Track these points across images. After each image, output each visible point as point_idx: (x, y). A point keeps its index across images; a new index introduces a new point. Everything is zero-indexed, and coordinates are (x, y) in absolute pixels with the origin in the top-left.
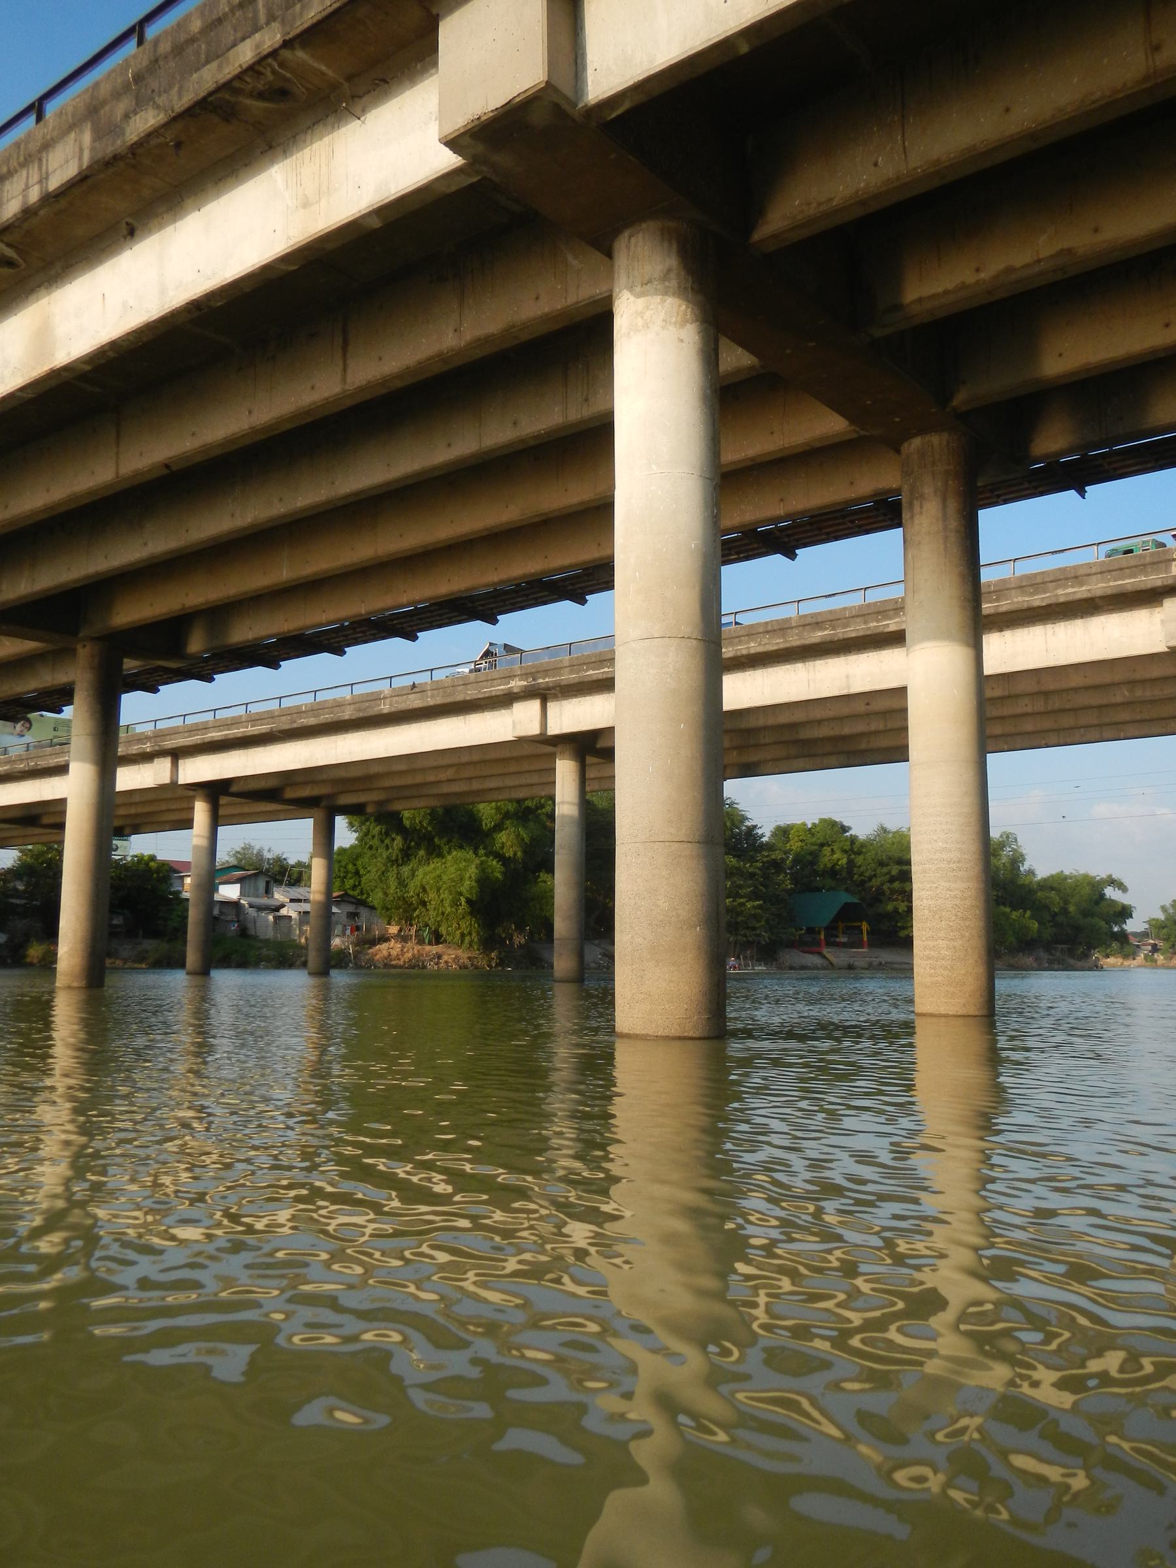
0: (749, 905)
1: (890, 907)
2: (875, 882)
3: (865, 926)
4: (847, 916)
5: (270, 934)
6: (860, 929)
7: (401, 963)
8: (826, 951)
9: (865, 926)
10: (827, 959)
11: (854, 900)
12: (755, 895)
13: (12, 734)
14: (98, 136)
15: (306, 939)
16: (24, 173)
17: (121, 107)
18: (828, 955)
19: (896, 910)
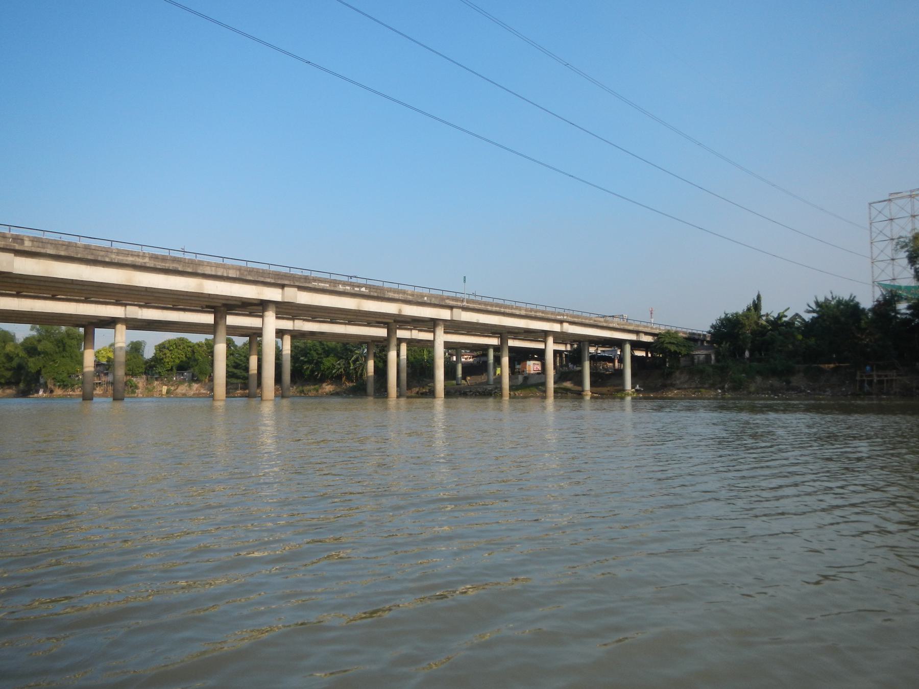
14: (241, 274)
16: (222, 270)
17: (245, 273)
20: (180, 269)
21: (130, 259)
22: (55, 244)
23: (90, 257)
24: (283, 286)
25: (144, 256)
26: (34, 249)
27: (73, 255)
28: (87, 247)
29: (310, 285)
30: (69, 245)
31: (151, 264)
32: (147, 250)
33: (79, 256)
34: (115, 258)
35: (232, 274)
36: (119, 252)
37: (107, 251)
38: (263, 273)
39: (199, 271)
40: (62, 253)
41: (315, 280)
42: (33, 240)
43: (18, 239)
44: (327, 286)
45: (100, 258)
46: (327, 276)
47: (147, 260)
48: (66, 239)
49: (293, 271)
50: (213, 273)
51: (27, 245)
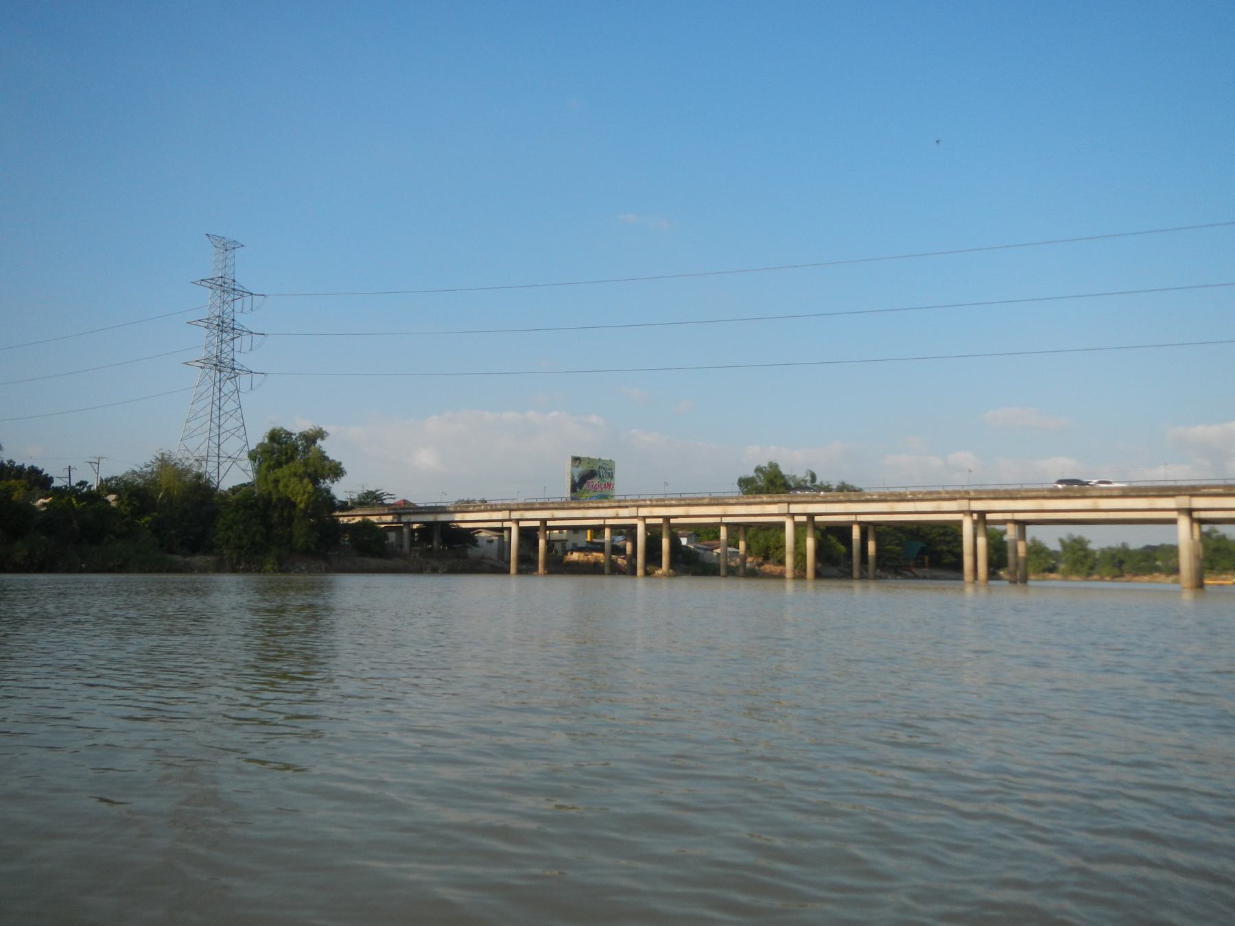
0: (897, 548)
1: (939, 548)
2: (930, 536)
3: (927, 558)
4: (923, 552)
5: (715, 561)
6: (924, 559)
7: (776, 574)
8: (913, 570)
9: (927, 558)
10: (913, 573)
11: (924, 545)
12: (897, 545)
13: (575, 466)
15: (736, 563)
18: (915, 572)
19: (942, 550)
20: (1071, 494)
21: (1034, 494)
22: (987, 492)
23: (1008, 496)
24: (1173, 496)
25: (1043, 490)
26: (976, 496)
27: (997, 496)
28: (1006, 491)
29: (1199, 493)
30: (995, 491)
31: (1049, 494)
32: (1045, 486)
33: (1002, 496)
34: (1024, 494)
35: (1115, 493)
36: (1027, 491)
37: (1018, 491)
38: (1146, 489)
39: (1087, 494)
40: (991, 496)
41: (1205, 487)
42: (975, 491)
43: (967, 492)
44: (1220, 491)
45: (1014, 496)
46: (1221, 483)
47: (1046, 493)
48: (993, 488)
49: (1179, 484)
50: (1098, 494)
51: (972, 495)
